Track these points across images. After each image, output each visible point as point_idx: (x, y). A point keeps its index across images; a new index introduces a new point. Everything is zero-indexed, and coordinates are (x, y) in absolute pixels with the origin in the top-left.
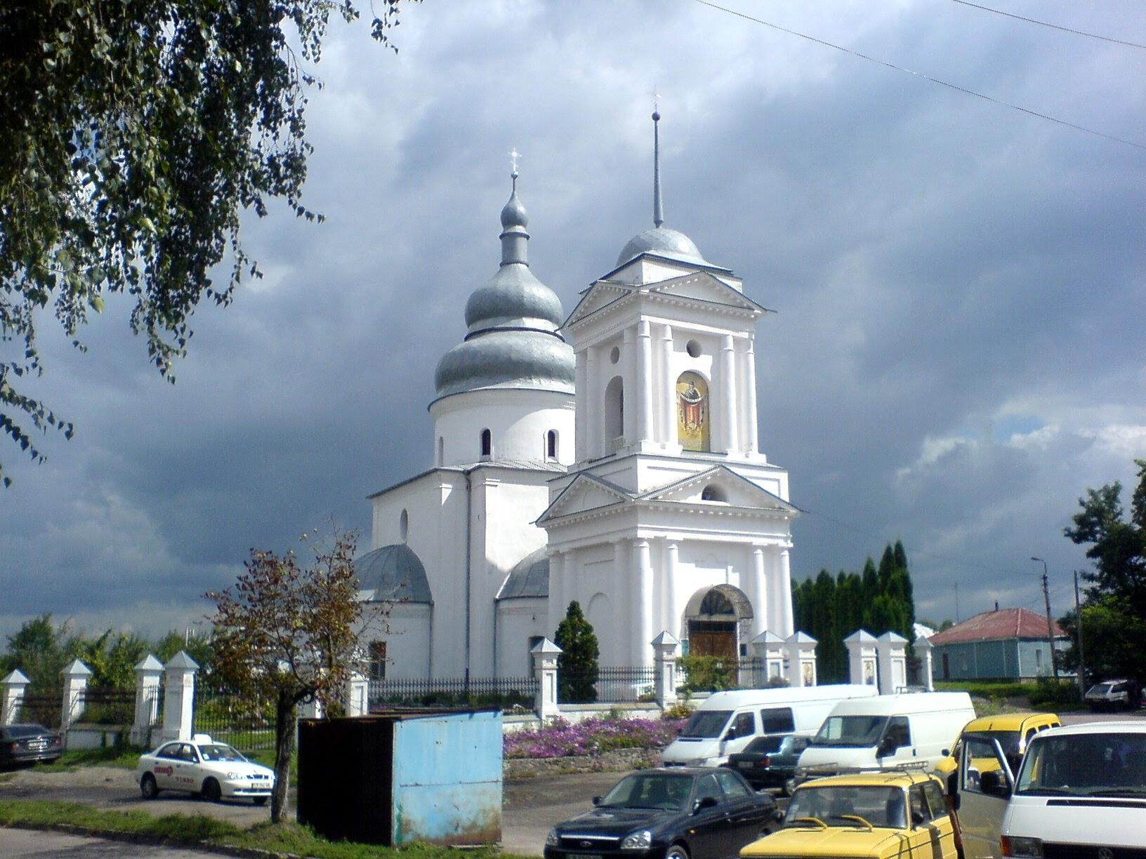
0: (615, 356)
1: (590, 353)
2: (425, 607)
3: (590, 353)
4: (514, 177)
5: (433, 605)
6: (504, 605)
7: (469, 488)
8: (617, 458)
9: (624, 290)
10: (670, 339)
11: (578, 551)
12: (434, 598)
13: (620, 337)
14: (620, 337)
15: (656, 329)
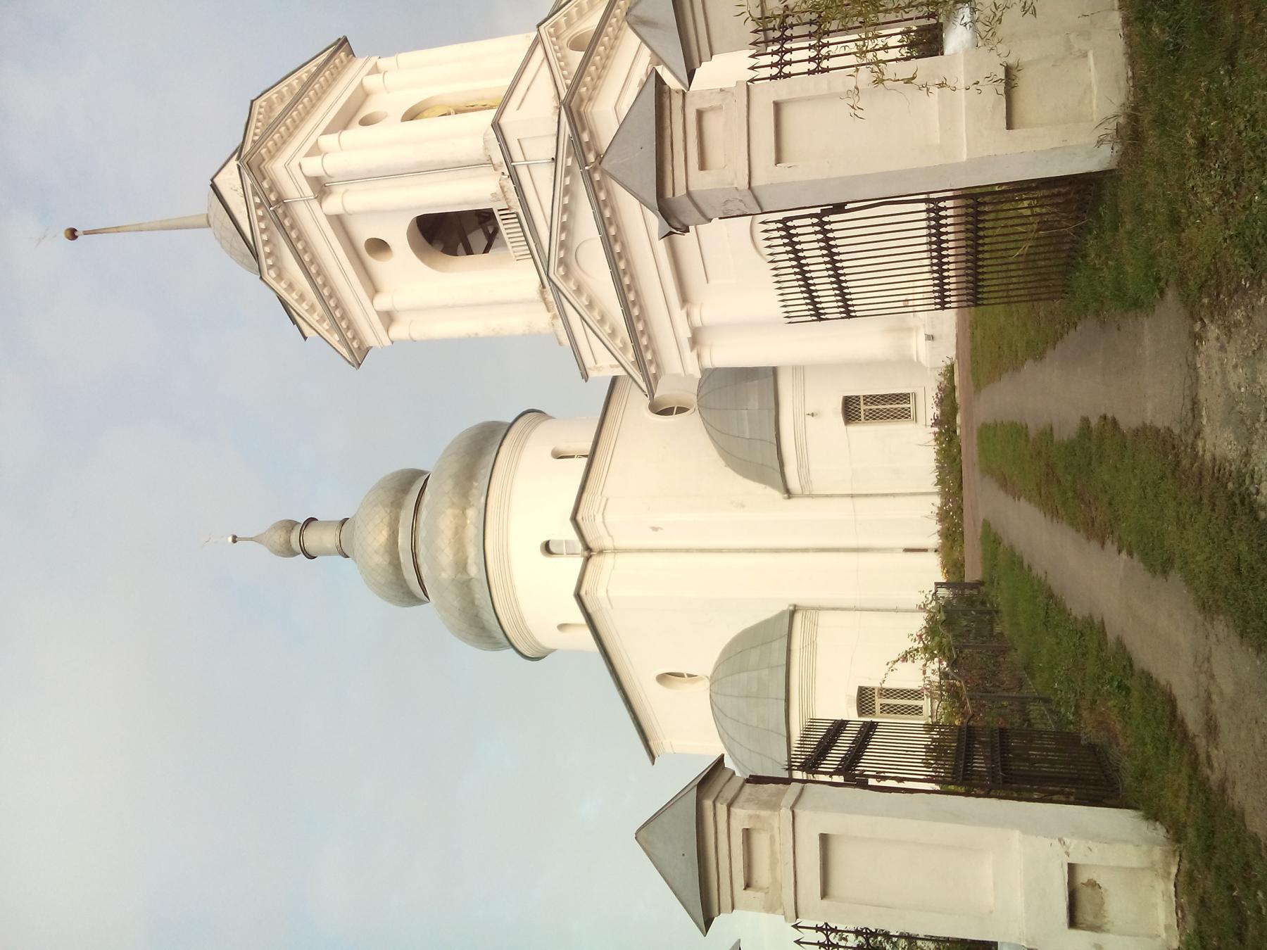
0: (379, 246)
1: (383, 302)
2: (798, 617)
3: (383, 302)
4: (235, 539)
5: (795, 606)
6: (794, 483)
7: (616, 551)
8: (520, 211)
9: (258, 206)
10: (337, 135)
11: (684, 299)
12: (785, 607)
13: (339, 223)
14: (339, 223)
15: (315, 151)
